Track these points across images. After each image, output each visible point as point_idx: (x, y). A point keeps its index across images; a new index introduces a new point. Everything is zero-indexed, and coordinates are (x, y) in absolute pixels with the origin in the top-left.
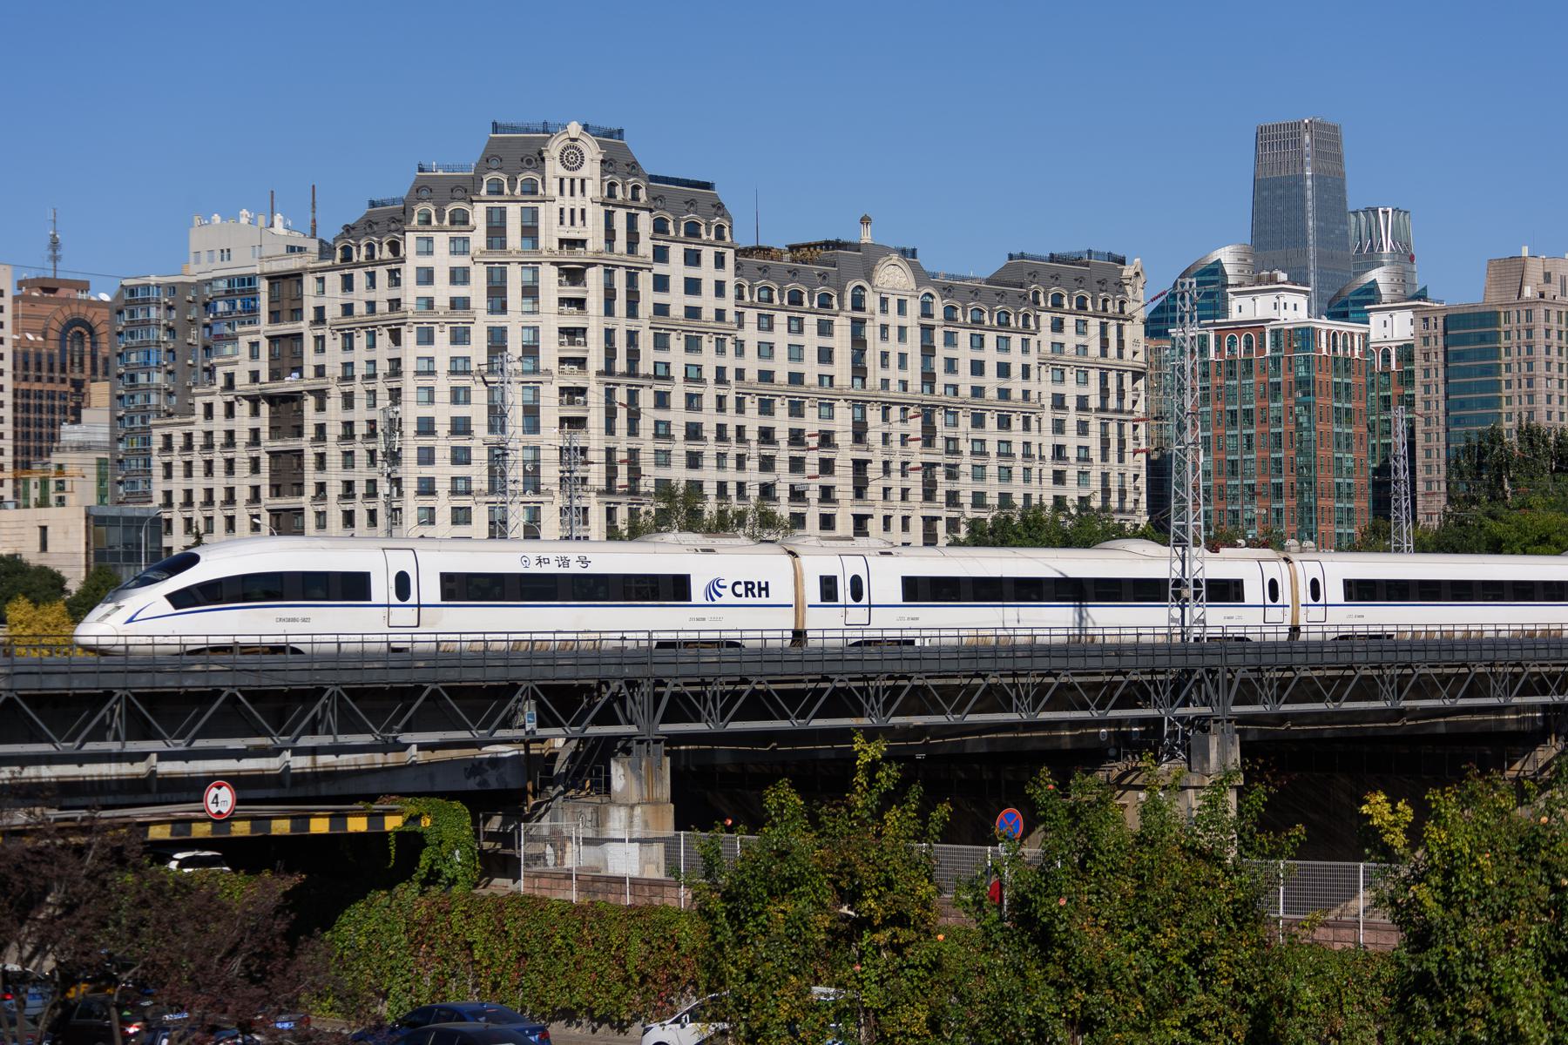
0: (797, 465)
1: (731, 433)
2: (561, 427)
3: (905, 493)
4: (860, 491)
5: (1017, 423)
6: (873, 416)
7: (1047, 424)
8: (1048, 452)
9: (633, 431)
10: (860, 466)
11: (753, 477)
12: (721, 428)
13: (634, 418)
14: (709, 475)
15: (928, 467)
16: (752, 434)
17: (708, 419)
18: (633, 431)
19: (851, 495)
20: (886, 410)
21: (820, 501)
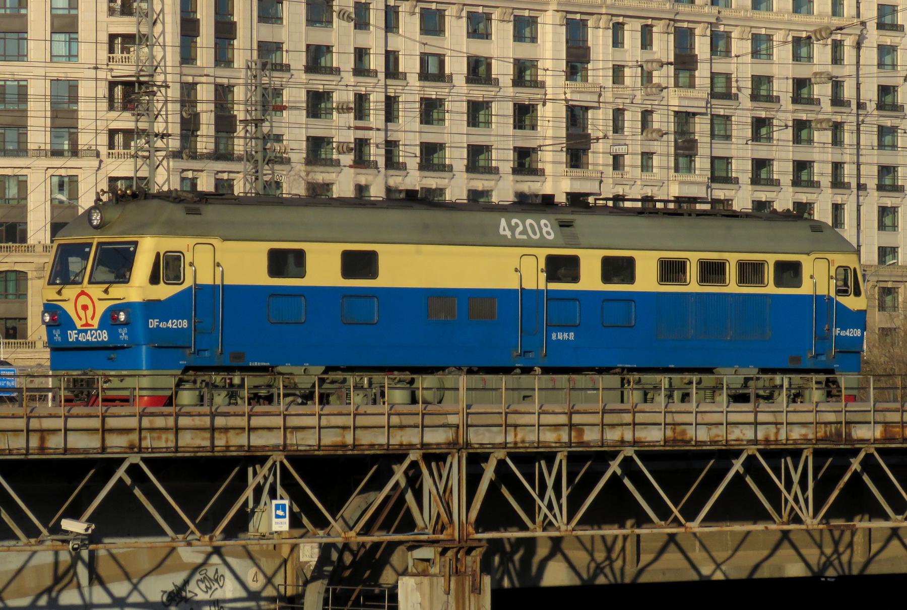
0: (477, 112)
1: (376, 62)
2: (111, 50)
3: (647, 156)
4: (576, 155)
5: (821, 53)
6: (598, 40)
7: (870, 55)
8: (870, 94)
9: (223, 58)
10: (576, 116)
11: (410, 132)
12: (361, 54)
13: (225, 31)
14: (340, 128)
15: (684, 118)
16: (409, 65)
17: (341, 37)
18: (223, 58)
19: (563, 157)
20: (618, 29)
21: (515, 171)
